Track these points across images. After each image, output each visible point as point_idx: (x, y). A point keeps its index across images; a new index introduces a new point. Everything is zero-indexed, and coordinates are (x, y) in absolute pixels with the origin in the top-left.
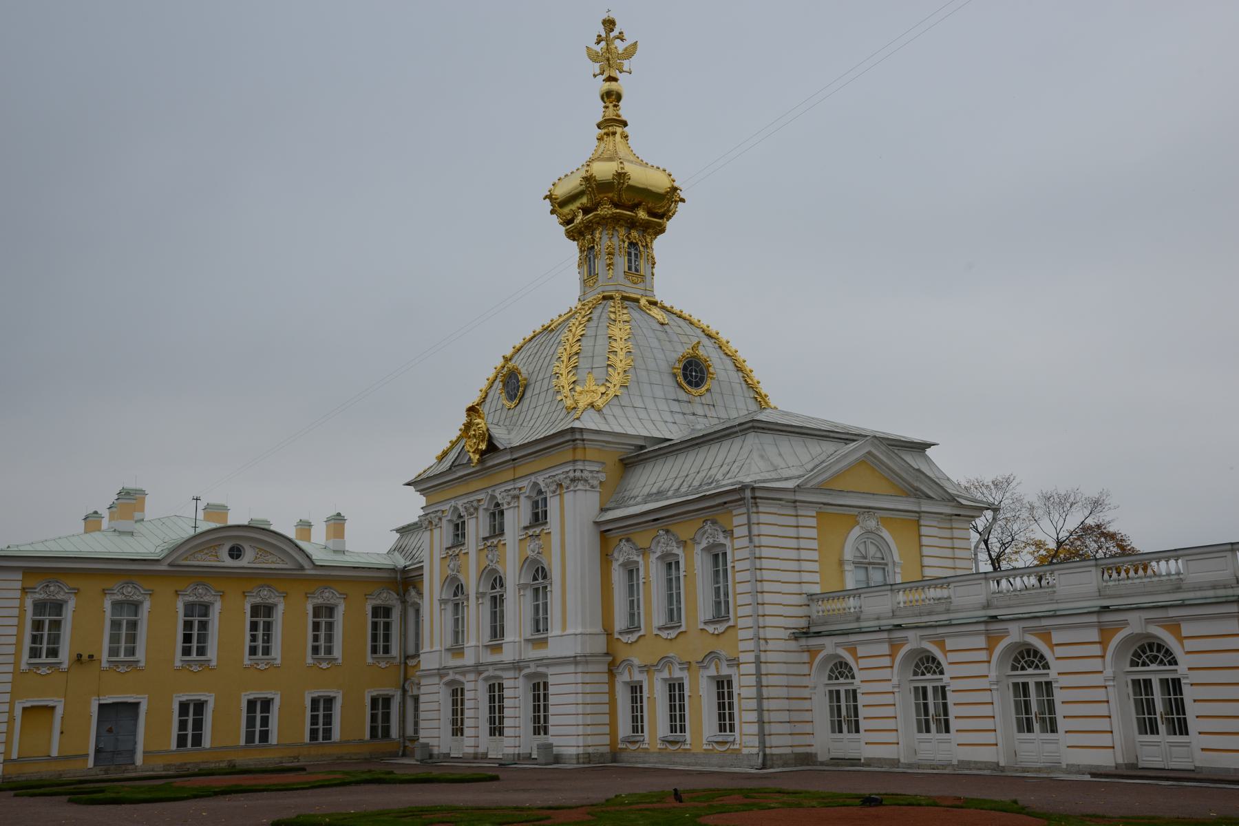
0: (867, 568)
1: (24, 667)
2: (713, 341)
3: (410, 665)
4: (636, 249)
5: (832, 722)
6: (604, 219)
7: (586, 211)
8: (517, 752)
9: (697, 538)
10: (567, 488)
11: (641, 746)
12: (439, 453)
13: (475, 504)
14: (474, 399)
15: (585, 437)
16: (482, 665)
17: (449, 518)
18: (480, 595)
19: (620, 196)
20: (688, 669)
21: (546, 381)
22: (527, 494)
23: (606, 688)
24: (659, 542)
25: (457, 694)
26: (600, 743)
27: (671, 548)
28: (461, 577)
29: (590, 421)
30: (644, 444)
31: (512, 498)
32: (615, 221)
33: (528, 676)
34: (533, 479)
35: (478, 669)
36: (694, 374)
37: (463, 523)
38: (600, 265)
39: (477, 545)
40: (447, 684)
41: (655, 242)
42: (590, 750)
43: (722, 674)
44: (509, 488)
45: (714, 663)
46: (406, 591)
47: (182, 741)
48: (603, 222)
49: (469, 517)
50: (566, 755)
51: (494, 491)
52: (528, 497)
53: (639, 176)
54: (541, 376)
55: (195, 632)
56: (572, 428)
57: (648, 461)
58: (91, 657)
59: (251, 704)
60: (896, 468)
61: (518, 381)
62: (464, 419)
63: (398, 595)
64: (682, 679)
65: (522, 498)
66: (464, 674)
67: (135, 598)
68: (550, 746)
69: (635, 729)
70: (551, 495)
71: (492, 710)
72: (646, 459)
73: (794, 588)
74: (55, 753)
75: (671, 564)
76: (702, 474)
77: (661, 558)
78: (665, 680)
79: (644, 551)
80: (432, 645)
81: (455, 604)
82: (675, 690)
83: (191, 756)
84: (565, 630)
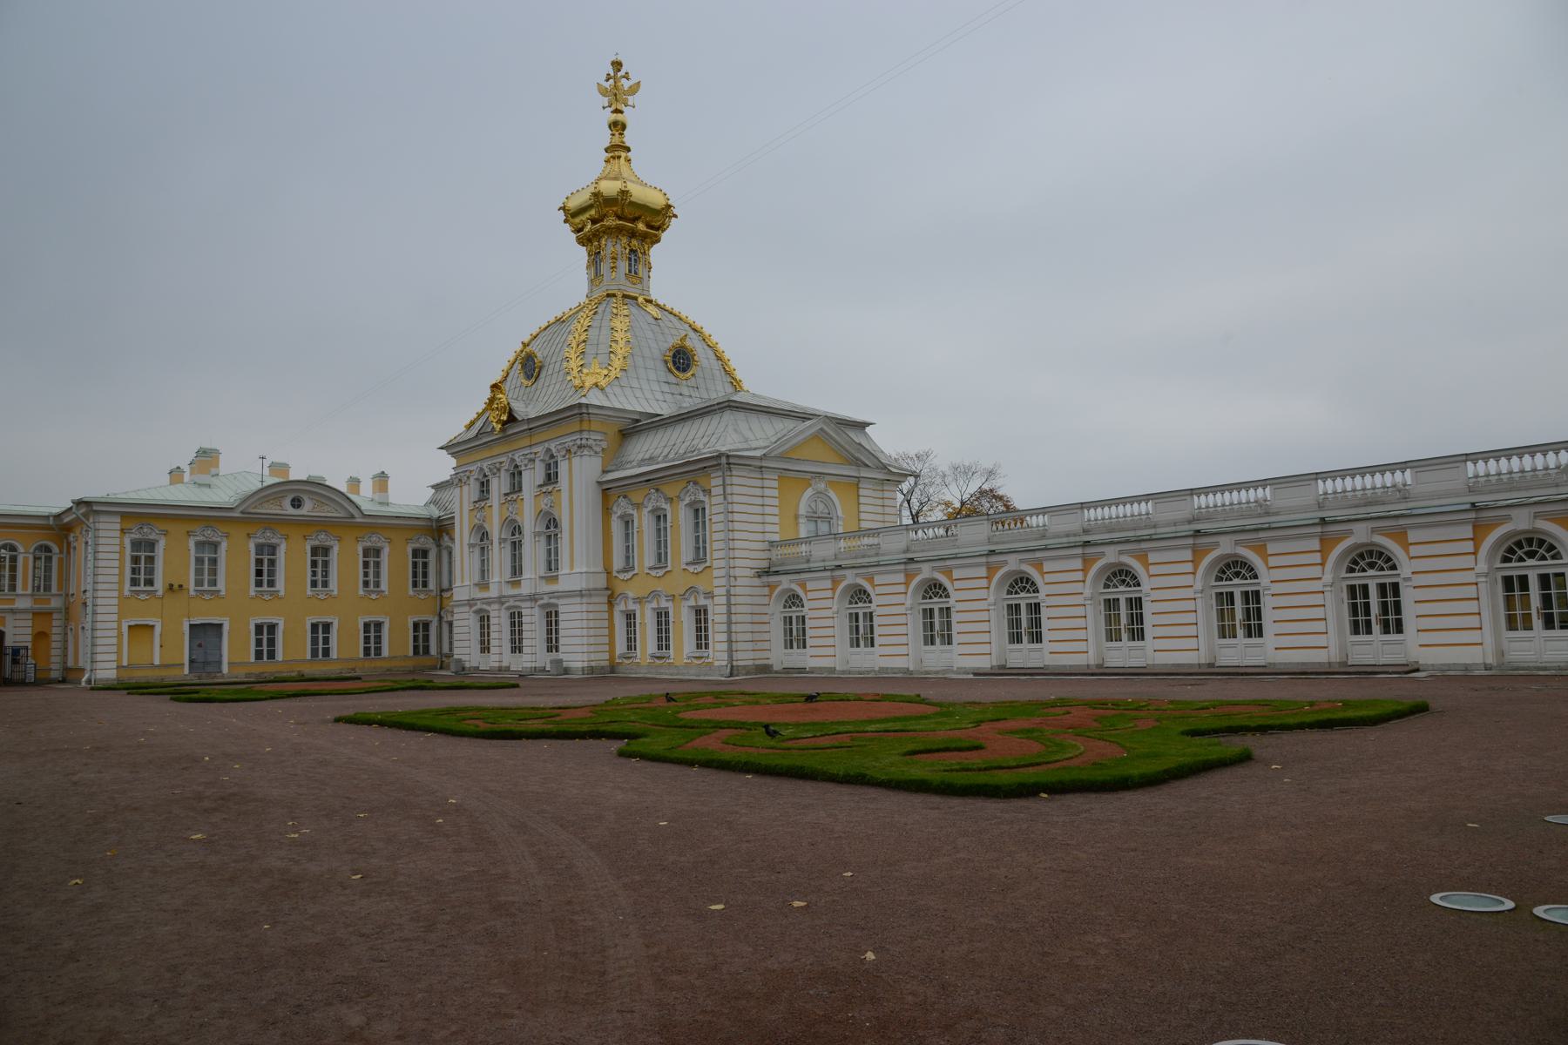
0: (816, 521)
1: (127, 593)
2: (698, 334)
5: (786, 641)
9: (682, 495)
10: (575, 453)
12: (467, 422)
13: (498, 465)
14: (497, 378)
15: (590, 411)
16: (505, 597)
17: (475, 477)
18: (502, 541)
19: (623, 210)
20: (673, 600)
21: (558, 364)
23: (606, 616)
25: (484, 620)
26: (602, 659)
28: (486, 525)
29: (594, 398)
32: (619, 230)
33: (542, 606)
34: (546, 445)
35: (500, 600)
37: (488, 481)
38: (605, 267)
39: (500, 500)
40: (475, 612)
41: (652, 250)
42: (593, 664)
45: (693, 596)
46: (440, 537)
47: (259, 655)
48: (609, 231)
53: (639, 193)
54: (553, 360)
55: (265, 568)
56: (579, 404)
58: (181, 586)
59: (314, 627)
60: (843, 443)
61: (534, 363)
62: (488, 394)
64: (667, 608)
65: (537, 460)
66: (489, 604)
67: (214, 539)
68: (561, 661)
69: (629, 648)
71: (513, 632)
73: (759, 537)
74: (157, 662)
75: (660, 517)
76: (687, 444)
77: (652, 511)
78: (654, 609)
79: (638, 506)
82: (662, 617)
83: (266, 668)
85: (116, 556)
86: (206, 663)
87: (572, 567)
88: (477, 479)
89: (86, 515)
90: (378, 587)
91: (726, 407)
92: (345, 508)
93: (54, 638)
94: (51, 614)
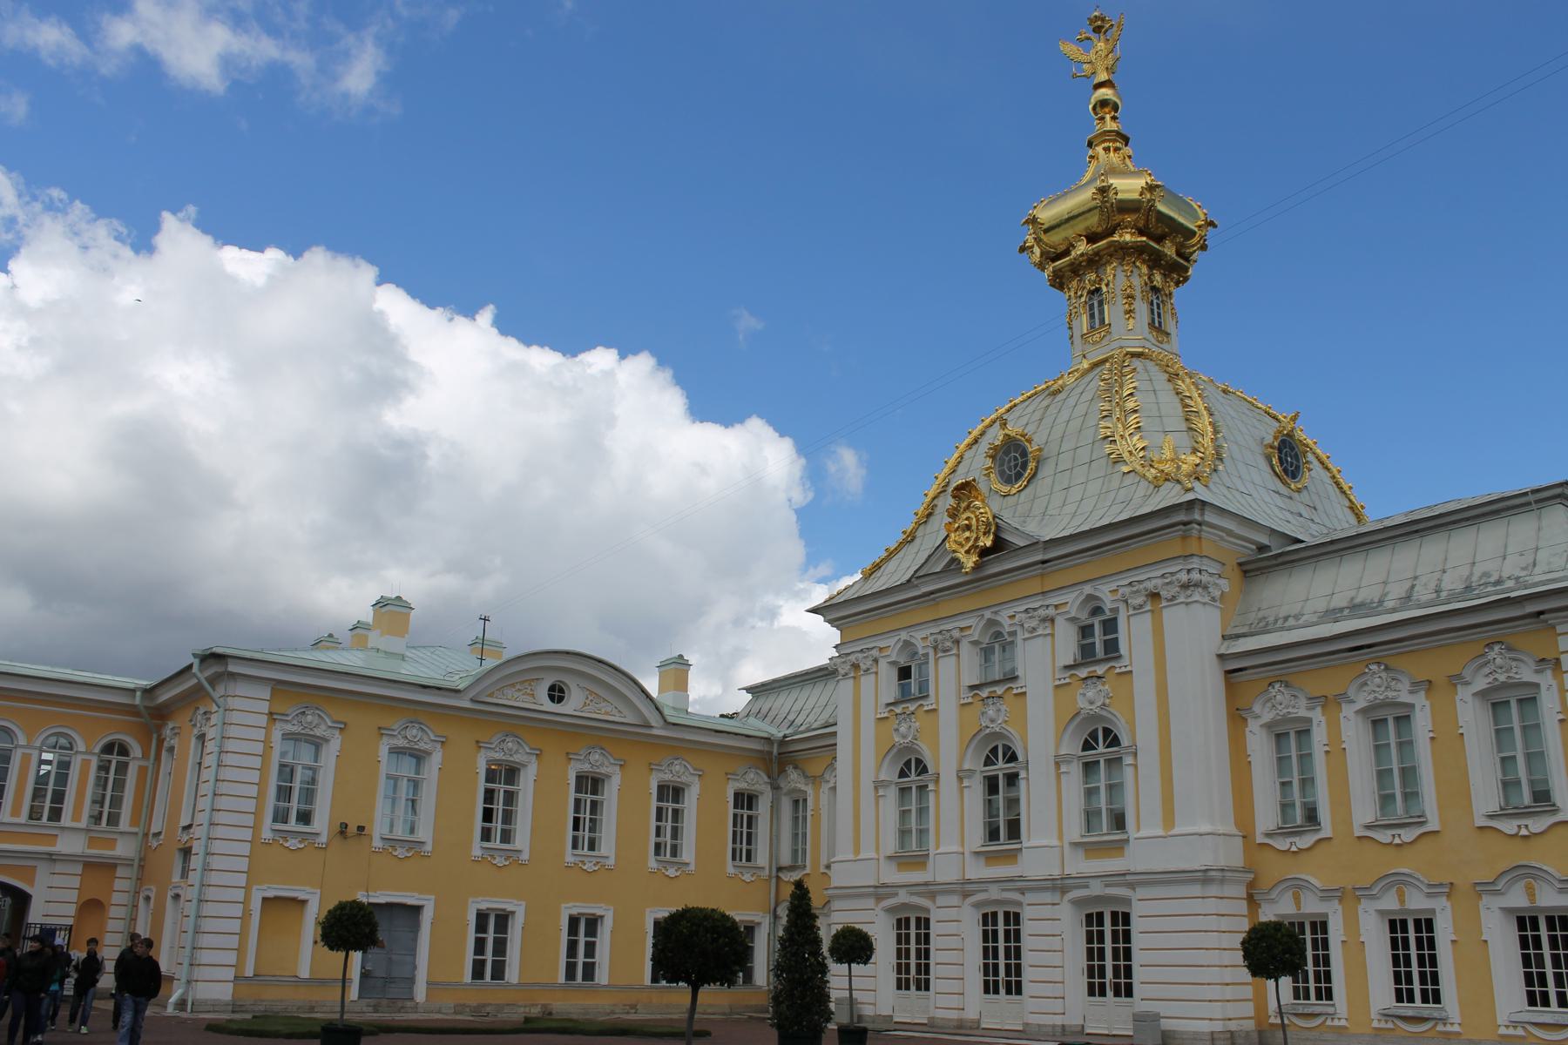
1: (267, 834)
3: (786, 880)
4: (1158, 298)
6: (1122, 248)
7: (1092, 238)
8: (1060, 1023)
9: (1351, 693)
11: (1329, 1023)
13: (956, 634)
16: (970, 882)
20: (1449, 896)
22: (1073, 614)
24: (1365, 684)
27: (1395, 694)
30: (1268, 544)
31: (1040, 621)
33: (1077, 903)
36: (1289, 459)
40: (890, 910)
42: (1233, 1026)
44: (1036, 605)
46: (782, 771)
47: (478, 971)
48: (1122, 252)
49: (940, 655)
50: (1182, 1032)
52: (1073, 620)
55: (499, 807)
58: (361, 828)
59: (574, 922)
63: (769, 777)
65: (1060, 621)
70: (1131, 612)
72: (1293, 561)
74: (305, 973)
78: (1381, 913)
79: (1330, 703)
81: (900, 789)
83: (488, 995)
84: (1173, 827)
85: (257, 762)
86: (389, 980)
87: (1169, 819)
89: (213, 680)
90: (675, 856)
91: (1558, 496)
92: (639, 710)
93: (114, 912)
94: (114, 866)
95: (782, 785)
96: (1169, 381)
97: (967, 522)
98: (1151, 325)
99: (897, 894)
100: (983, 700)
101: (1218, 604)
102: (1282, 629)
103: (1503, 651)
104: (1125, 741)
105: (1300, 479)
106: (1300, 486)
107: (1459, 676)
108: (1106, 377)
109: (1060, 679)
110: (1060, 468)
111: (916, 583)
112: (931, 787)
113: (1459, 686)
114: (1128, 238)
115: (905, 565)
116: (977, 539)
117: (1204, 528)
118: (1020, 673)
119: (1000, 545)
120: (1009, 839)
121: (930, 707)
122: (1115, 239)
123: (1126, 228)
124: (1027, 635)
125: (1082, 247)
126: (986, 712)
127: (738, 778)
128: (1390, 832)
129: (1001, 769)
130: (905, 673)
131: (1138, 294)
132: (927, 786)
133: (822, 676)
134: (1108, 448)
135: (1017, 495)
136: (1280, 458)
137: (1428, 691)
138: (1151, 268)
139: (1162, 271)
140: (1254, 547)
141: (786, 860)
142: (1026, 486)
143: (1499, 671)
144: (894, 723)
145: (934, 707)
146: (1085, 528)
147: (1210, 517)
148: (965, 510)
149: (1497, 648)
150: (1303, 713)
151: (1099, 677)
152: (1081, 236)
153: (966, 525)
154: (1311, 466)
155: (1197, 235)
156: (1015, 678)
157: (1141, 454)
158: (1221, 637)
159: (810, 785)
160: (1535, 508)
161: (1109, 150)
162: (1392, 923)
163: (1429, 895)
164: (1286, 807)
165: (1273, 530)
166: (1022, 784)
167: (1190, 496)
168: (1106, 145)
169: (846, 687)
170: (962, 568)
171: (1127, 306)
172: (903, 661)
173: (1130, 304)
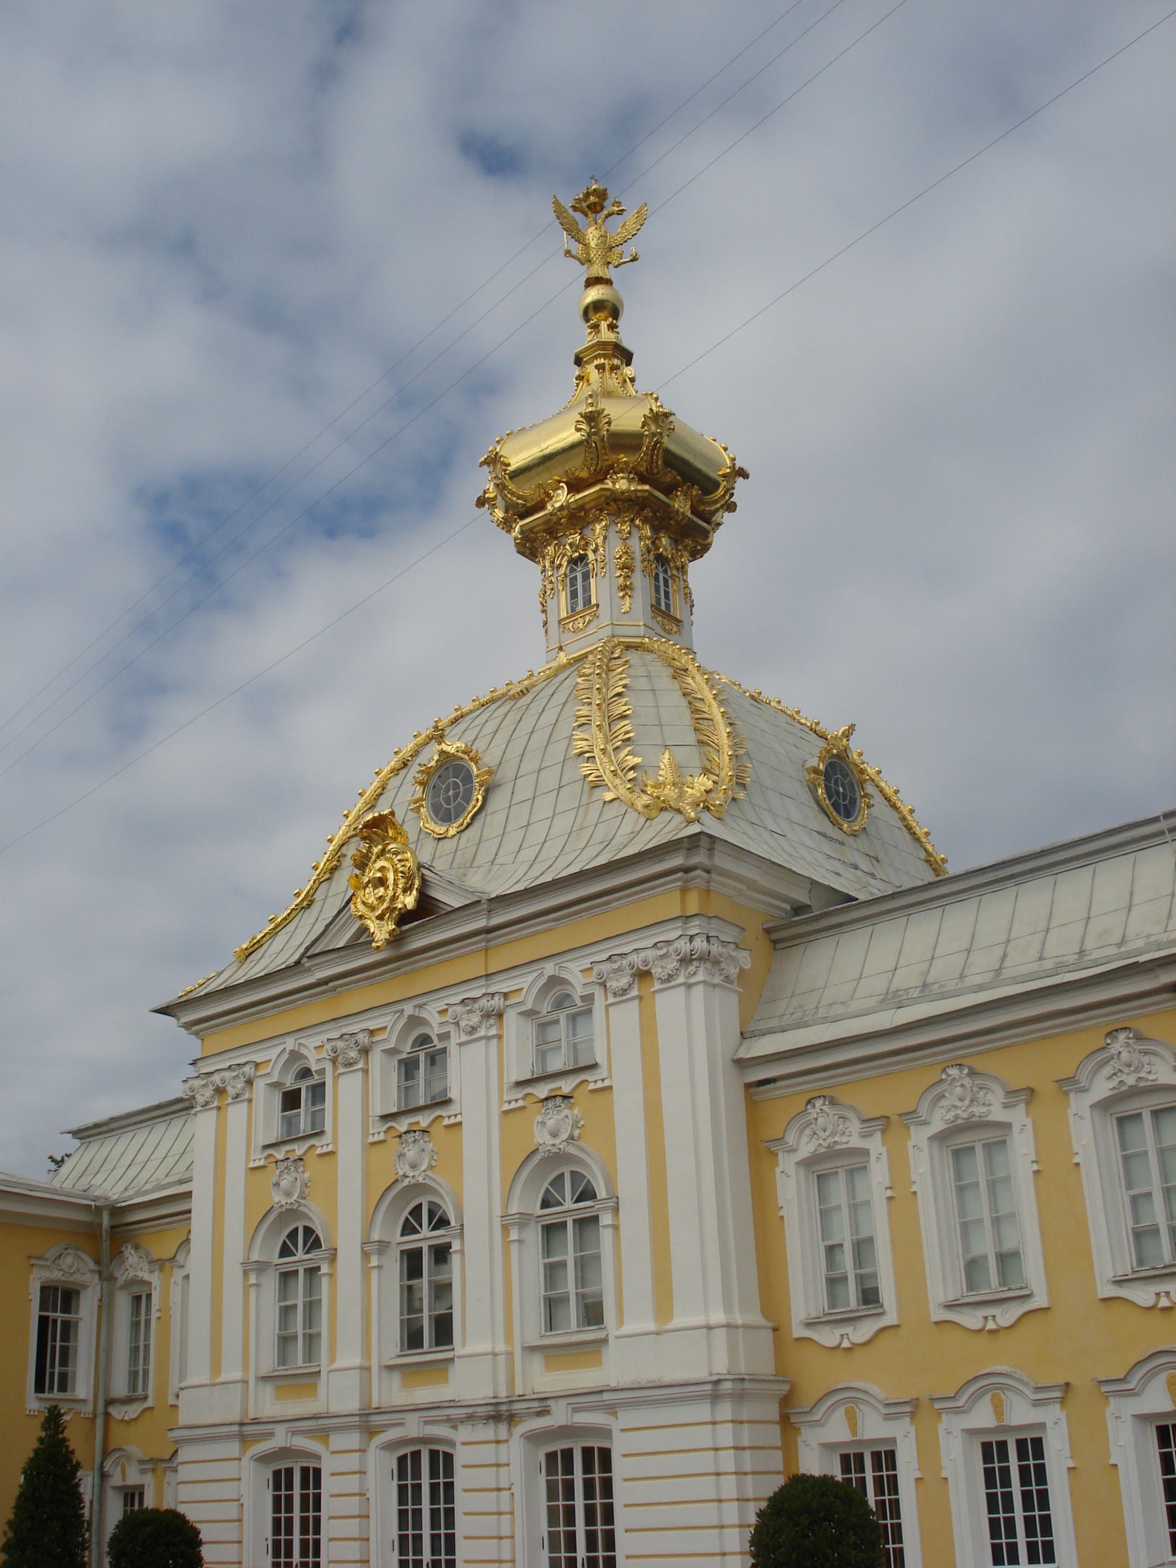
3: (119, 1417)
4: (665, 572)
6: (615, 500)
9: (923, 1112)
13: (363, 1039)
16: (380, 1411)
20: (1062, 1401)
24: (941, 1096)
27: (984, 1109)
30: (808, 902)
31: (483, 1017)
33: (535, 1438)
36: (841, 790)
39: (365, 1132)
43: (1012, 1424)
46: (117, 1253)
48: (617, 506)
49: (341, 1070)
51: (420, 1006)
57: (845, 929)
65: (511, 1017)
70: (611, 1000)
72: (841, 925)
78: (971, 1433)
80: (216, 1366)
88: (275, 1085)
95: (117, 1274)
96: (674, 678)
97: (379, 875)
98: (656, 608)
99: (272, 1434)
100: (400, 1136)
101: (734, 987)
102: (825, 1020)
103: (1131, 1041)
104: (602, 1193)
105: (856, 818)
106: (857, 828)
107: (1071, 1080)
108: (587, 671)
109: (510, 1102)
110: (516, 799)
111: (306, 965)
112: (325, 1269)
113: (1072, 1095)
114: (622, 485)
115: (297, 941)
116: (394, 898)
117: (714, 876)
118: (453, 1094)
119: (426, 908)
120: (437, 1344)
121: (325, 1150)
122: (606, 486)
123: (622, 471)
124: (464, 1038)
125: (562, 497)
126: (405, 1155)
127: (48, 1263)
128: (981, 1313)
129: (426, 1237)
130: (291, 1100)
131: (638, 565)
132: (319, 1268)
133: (181, 1110)
134: (585, 768)
135: (456, 838)
136: (828, 790)
137: (1028, 1103)
138: (656, 530)
139: (672, 536)
140: (788, 907)
141: (120, 1388)
142: (469, 825)
143: (1126, 1070)
144: (274, 1173)
145: (330, 1148)
146: (547, 878)
147: (721, 861)
148: (378, 857)
149: (1122, 1036)
150: (856, 1142)
151: (565, 1097)
152: (560, 482)
153: (379, 877)
154: (872, 802)
155: (721, 488)
156: (447, 1102)
157: (631, 775)
158: (739, 1034)
159: (156, 1273)
160: (1169, 839)
161: (604, 369)
162: (986, 1448)
163: (1037, 1403)
164: (834, 1282)
165: (814, 883)
166: (455, 1259)
167: (694, 829)
168: (596, 362)
169: (204, 1123)
170: (373, 941)
171: (622, 579)
172: (290, 1083)
173: (627, 577)
